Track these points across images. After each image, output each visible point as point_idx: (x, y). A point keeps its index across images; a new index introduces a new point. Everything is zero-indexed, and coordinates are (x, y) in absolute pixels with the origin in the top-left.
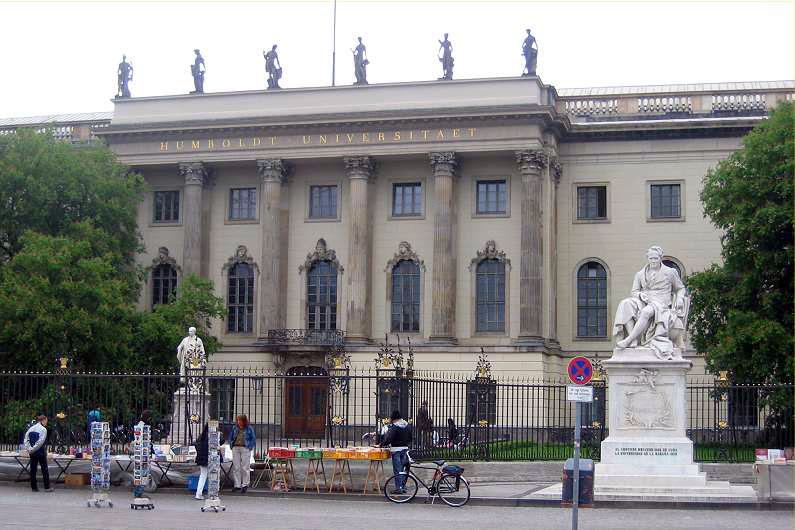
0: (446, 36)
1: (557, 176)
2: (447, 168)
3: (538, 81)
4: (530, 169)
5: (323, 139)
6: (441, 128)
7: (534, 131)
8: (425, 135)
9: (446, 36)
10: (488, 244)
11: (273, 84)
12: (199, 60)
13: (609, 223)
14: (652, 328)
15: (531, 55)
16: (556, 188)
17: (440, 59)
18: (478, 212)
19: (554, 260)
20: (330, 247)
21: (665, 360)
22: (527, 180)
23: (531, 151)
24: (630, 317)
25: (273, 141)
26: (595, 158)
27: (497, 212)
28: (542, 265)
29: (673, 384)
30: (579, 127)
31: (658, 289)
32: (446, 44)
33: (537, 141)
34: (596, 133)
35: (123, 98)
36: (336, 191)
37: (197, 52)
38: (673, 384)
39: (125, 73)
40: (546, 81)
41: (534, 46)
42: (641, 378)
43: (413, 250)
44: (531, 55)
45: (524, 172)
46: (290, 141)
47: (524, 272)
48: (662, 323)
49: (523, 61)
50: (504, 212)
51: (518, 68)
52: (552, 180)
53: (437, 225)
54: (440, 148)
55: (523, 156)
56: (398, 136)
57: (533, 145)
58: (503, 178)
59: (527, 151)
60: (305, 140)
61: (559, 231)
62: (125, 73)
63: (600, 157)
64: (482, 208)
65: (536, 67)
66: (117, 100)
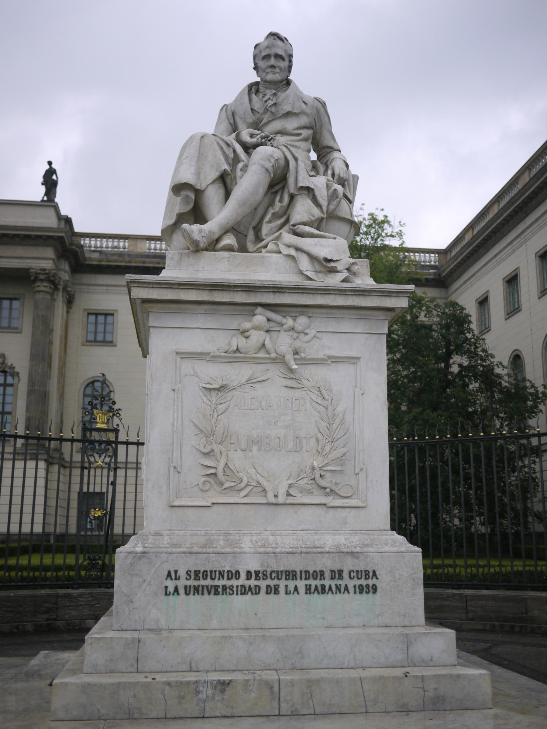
1: (70, 302)
4: (44, 286)
7: (50, 253)
13: (115, 346)
14: (278, 206)
16: (68, 312)
19: (62, 375)
21: (334, 280)
22: (39, 296)
23: (45, 270)
24: (214, 175)
26: (105, 288)
27: (9, 327)
28: (50, 379)
29: (353, 360)
30: (91, 259)
33: (51, 262)
34: (108, 266)
38: (353, 360)
40: (63, 212)
41: (54, 177)
42: (256, 337)
45: (38, 289)
47: (31, 383)
49: (43, 189)
50: (16, 328)
52: (63, 302)
55: (37, 274)
57: (48, 265)
58: (16, 296)
59: (41, 270)
61: (68, 351)
63: (110, 288)
65: (55, 197)
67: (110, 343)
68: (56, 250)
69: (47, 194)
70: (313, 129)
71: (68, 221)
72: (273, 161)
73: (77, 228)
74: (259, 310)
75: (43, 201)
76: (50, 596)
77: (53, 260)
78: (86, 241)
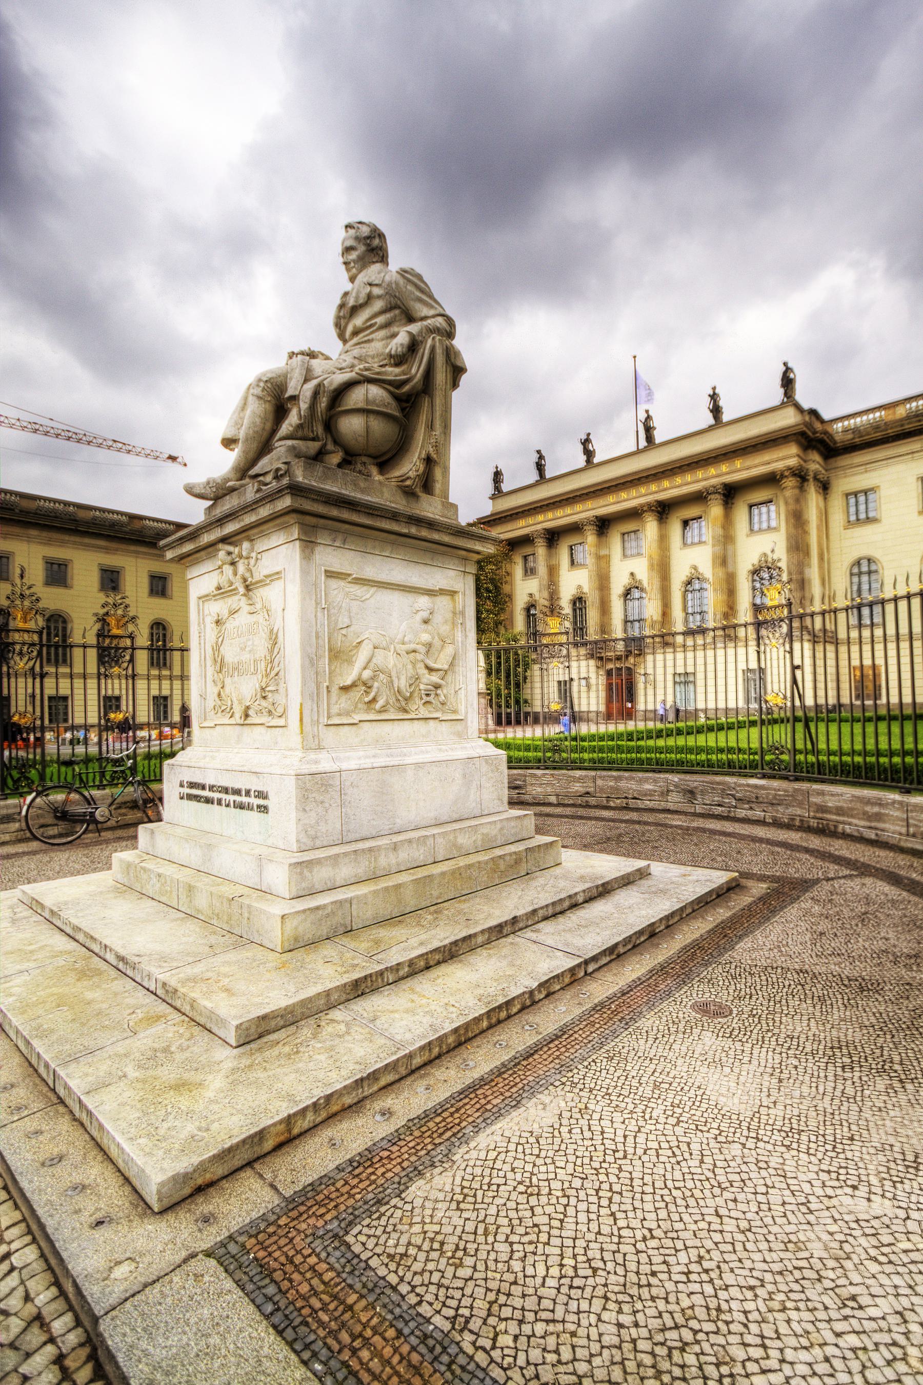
0: (714, 389)
2: (717, 496)
3: (797, 407)
5: (623, 495)
6: (711, 464)
8: (700, 474)
9: (714, 389)
10: (761, 556)
11: (589, 461)
12: (541, 457)
15: (788, 382)
17: (711, 411)
18: (751, 530)
20: (638, 577)
25: (589, 504)
31: (355, 333)
32: (714, 397)
35: (498, 493)
36: (641, 535)
37: (539, 452)
39: (497, 476)
40: (806, 405)
41: (792, 376)
43: (701, 570)
44: (788, 382)
46: (601, 501)
48: (294, 398)
51: (778, 395)
53: (713, 546)
54: (714, 481)
56: (678, 480)
57: (793, 462)
60: (611, 498)
62: (497, 476)
64: (756, 527)
66: (493, 497)
67: (875, 520)
68: (799, 444)
69: (786, 394)
70: (399, 308)
71: (814, 413)
72: (262, 384)
73: (826, 415)
74: (220, 546)
75: (783, 403)
76: (519, 775)
77: (798, 456)
78: (839, 426)
